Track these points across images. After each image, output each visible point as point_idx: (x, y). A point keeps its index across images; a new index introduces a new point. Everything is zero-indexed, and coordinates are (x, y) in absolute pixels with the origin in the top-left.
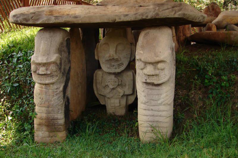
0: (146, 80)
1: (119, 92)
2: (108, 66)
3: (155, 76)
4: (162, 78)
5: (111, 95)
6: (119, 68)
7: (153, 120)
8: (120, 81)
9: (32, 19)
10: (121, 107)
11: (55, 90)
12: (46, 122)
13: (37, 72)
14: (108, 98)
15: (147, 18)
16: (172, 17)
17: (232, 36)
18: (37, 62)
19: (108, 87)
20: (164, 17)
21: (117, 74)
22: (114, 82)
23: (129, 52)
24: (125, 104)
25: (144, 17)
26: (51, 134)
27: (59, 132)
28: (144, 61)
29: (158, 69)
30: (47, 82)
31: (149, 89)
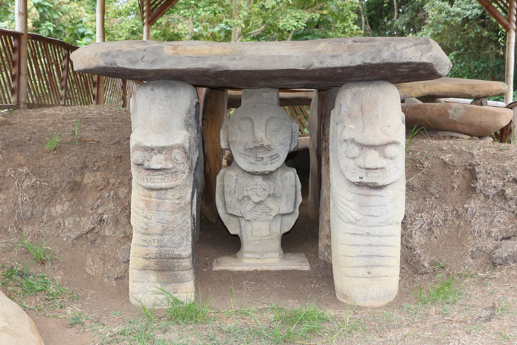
0: (360, 178)
1: (271, 209)
2: (253, 160)
3: (378, 171)
4: (391, 174)
5: (254, 215)
6: (271, 164)
7: (371, 254)
8: (272, 187)
9: (144, 60)
10: (272, 237)
11: (177, 202)
12: (157, 265)
13: (146, 165)
14: (248, 220)
15: (374, 62)
16: (418, 60)
17: (450, 111)
18: (148, 144)
19: (249, 199)
20: (405, 61)
21: (266, 175)
22: (262, 190)
23: (288, 134)
24: (279, 232)
25: (368, 61)
26: (168, 288)
27: (181, 282)
28: (360, 142)
29: (385, 157)
30: (163, 185)
31: (363, 195)
